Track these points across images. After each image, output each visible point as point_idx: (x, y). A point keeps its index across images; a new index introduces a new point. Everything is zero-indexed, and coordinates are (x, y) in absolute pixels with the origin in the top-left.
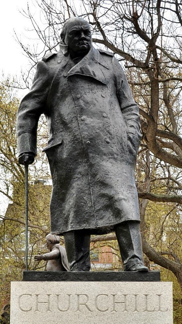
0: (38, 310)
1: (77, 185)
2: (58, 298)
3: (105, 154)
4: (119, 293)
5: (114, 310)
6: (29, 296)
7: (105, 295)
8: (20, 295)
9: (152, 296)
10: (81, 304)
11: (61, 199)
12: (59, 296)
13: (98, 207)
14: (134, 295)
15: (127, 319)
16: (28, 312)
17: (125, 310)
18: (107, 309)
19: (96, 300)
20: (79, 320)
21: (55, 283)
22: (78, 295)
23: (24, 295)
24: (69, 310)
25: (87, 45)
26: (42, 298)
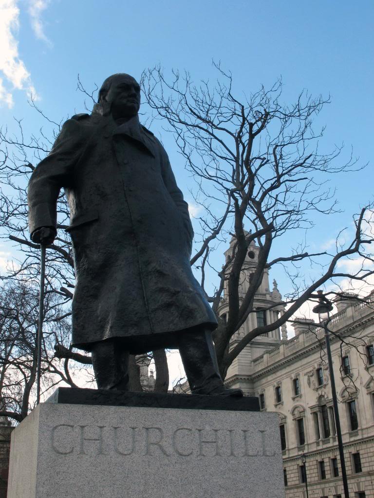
0: (85, 453)
1: (121, 275)
2: (115, 433)
4: (208, 428)
6: (69, 427)
8: (55, 426)
9: (252, 433)
10: (152, 444)
11: (91, 295)
12: (119, 429)
13: (153, 306)
14: (229, 430)
15: (221, 468)
16: (68, 455)
18: (191, 452)
19: (174, 437)
20: (150, 471)
21: (113, 408)
22: (147, 429)
23: (61, 425)
24: (134, 454)
26: (90, 433)
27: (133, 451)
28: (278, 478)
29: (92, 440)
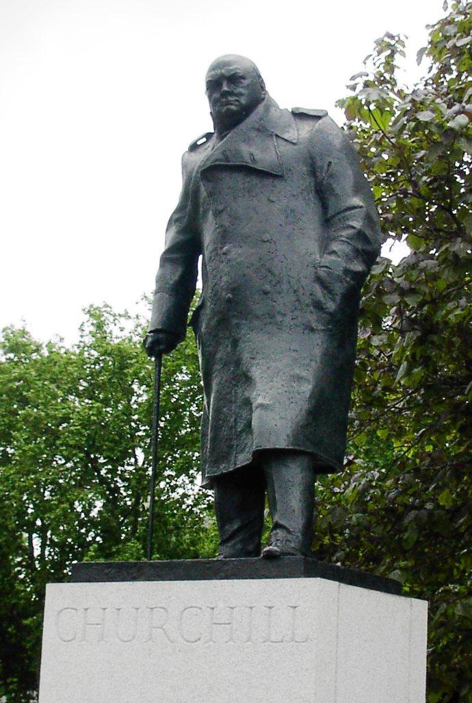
3: (257, 317)
4: (221, 605)
5: (211, 640)
7: (196, 607)
17: (231, 639)
18: (197, 637)
23: (65, 609)
25: (236, 103)
27: (134, 637)
28: (306, 674)
29: (93, 624)
